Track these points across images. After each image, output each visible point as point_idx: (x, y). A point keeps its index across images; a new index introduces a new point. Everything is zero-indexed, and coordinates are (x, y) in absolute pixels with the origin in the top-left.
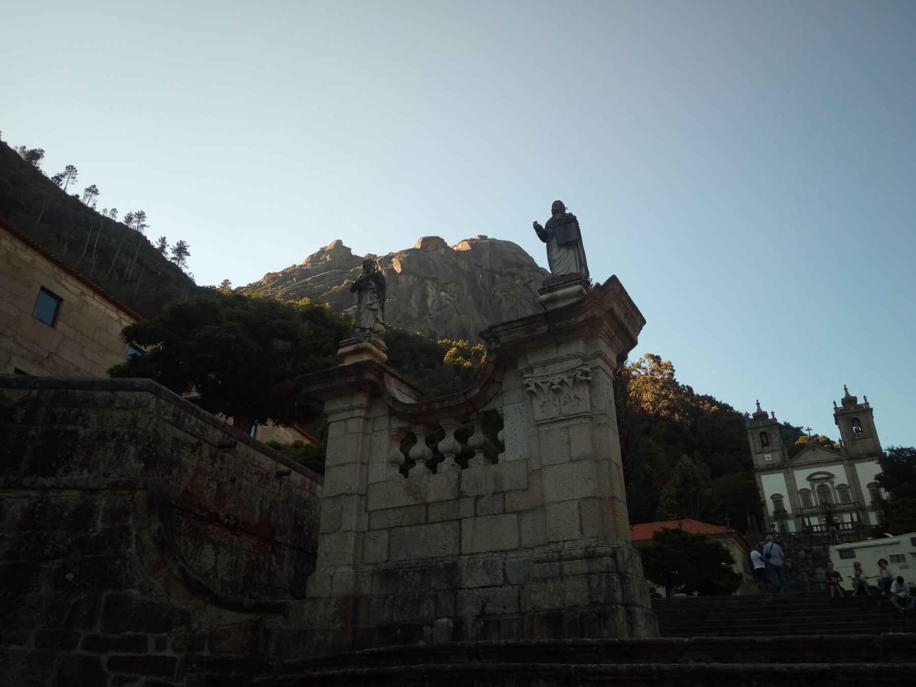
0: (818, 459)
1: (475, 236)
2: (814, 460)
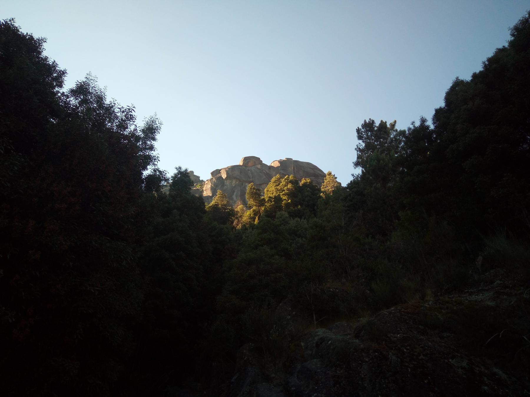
1: (284, 159)
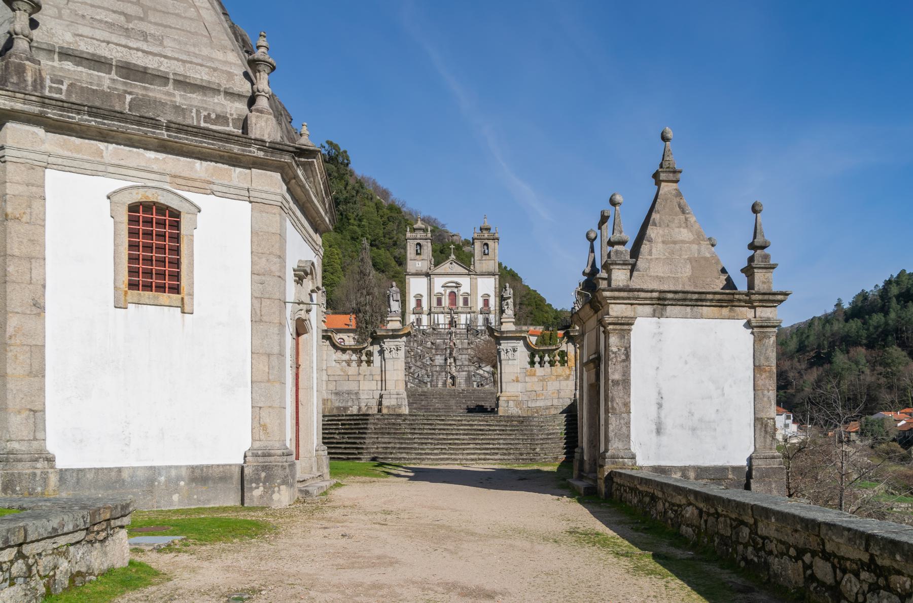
0: (454, 271)
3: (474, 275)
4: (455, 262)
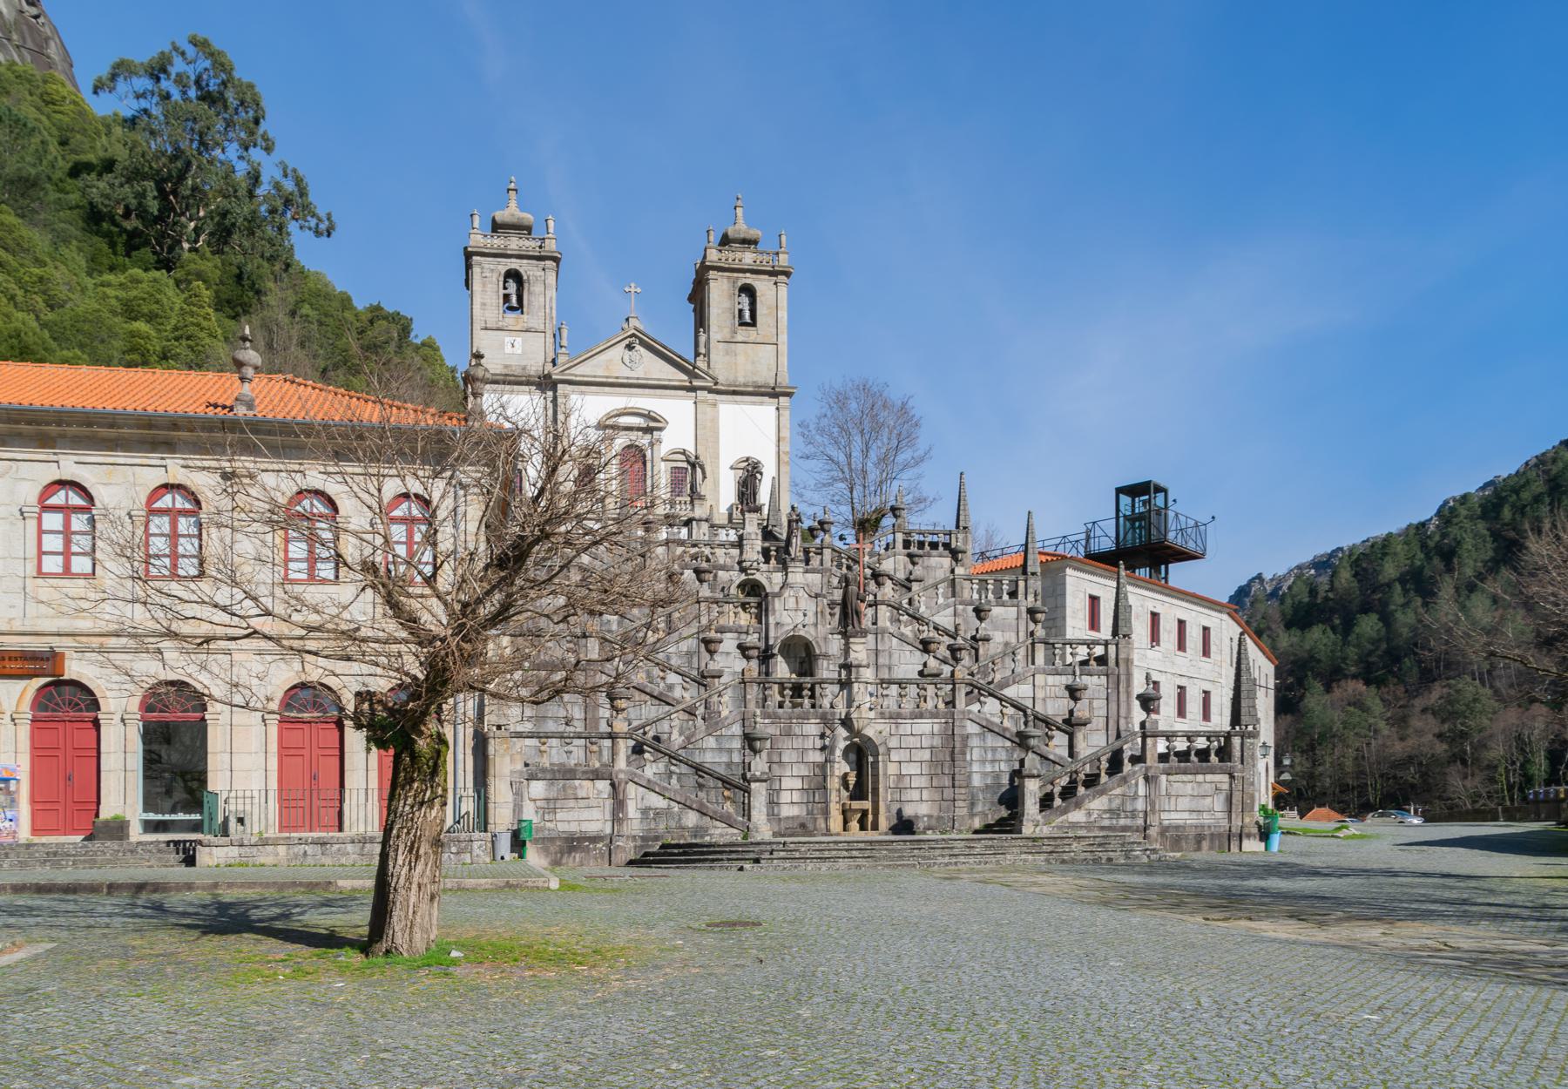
2: (627, 373)
3: (710, 391)
4: (643, 344)
